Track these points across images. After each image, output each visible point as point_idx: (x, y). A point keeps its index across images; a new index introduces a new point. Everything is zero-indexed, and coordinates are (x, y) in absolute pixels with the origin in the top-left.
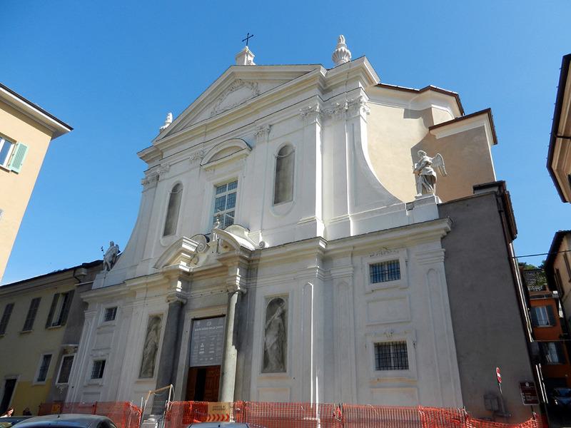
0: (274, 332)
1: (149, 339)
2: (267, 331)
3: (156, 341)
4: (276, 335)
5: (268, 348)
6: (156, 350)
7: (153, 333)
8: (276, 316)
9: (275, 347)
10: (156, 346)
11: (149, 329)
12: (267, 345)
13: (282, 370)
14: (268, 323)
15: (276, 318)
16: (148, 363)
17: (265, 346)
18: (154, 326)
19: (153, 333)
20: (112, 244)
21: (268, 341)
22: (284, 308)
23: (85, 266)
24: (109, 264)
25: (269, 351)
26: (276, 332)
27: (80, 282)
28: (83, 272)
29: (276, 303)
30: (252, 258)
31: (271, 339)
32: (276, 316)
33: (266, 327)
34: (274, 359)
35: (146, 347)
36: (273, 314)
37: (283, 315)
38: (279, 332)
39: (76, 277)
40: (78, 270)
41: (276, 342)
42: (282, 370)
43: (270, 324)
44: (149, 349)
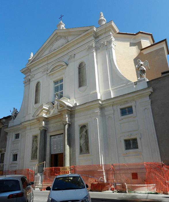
0: (83, 138)
1: (33, 145)
2: (81, 138)
4: (84, 140)
5: (82, 145)
6: (37, 148)
7: (35, 142)
8: (84, 132)
9: (84, 144)
10: (36, 147)
11: (33, 141)
12: (81, 144)
13: (88, 153)
17: (80, 144)
18: (35, 140)
19: (35, 142)
20: (14, 109)
21: (81, 142)
23: (4, 118)
24: (14, 117)
25: (82, 147)
26: (84, 139)
27: (3, 125)
28: (4, 120)
29: (83, 127)
30: (72, 110)
31: (83, 141)
32: (84, 132)
33: (80, 137)
34: (84, 148)
35: (33, 148)
38: (85, 138)
39: (1, 123)
40: (2, 120)
41: (84, 142)
42: (88, 153)
43: (82, 135)
44: (34, 148)
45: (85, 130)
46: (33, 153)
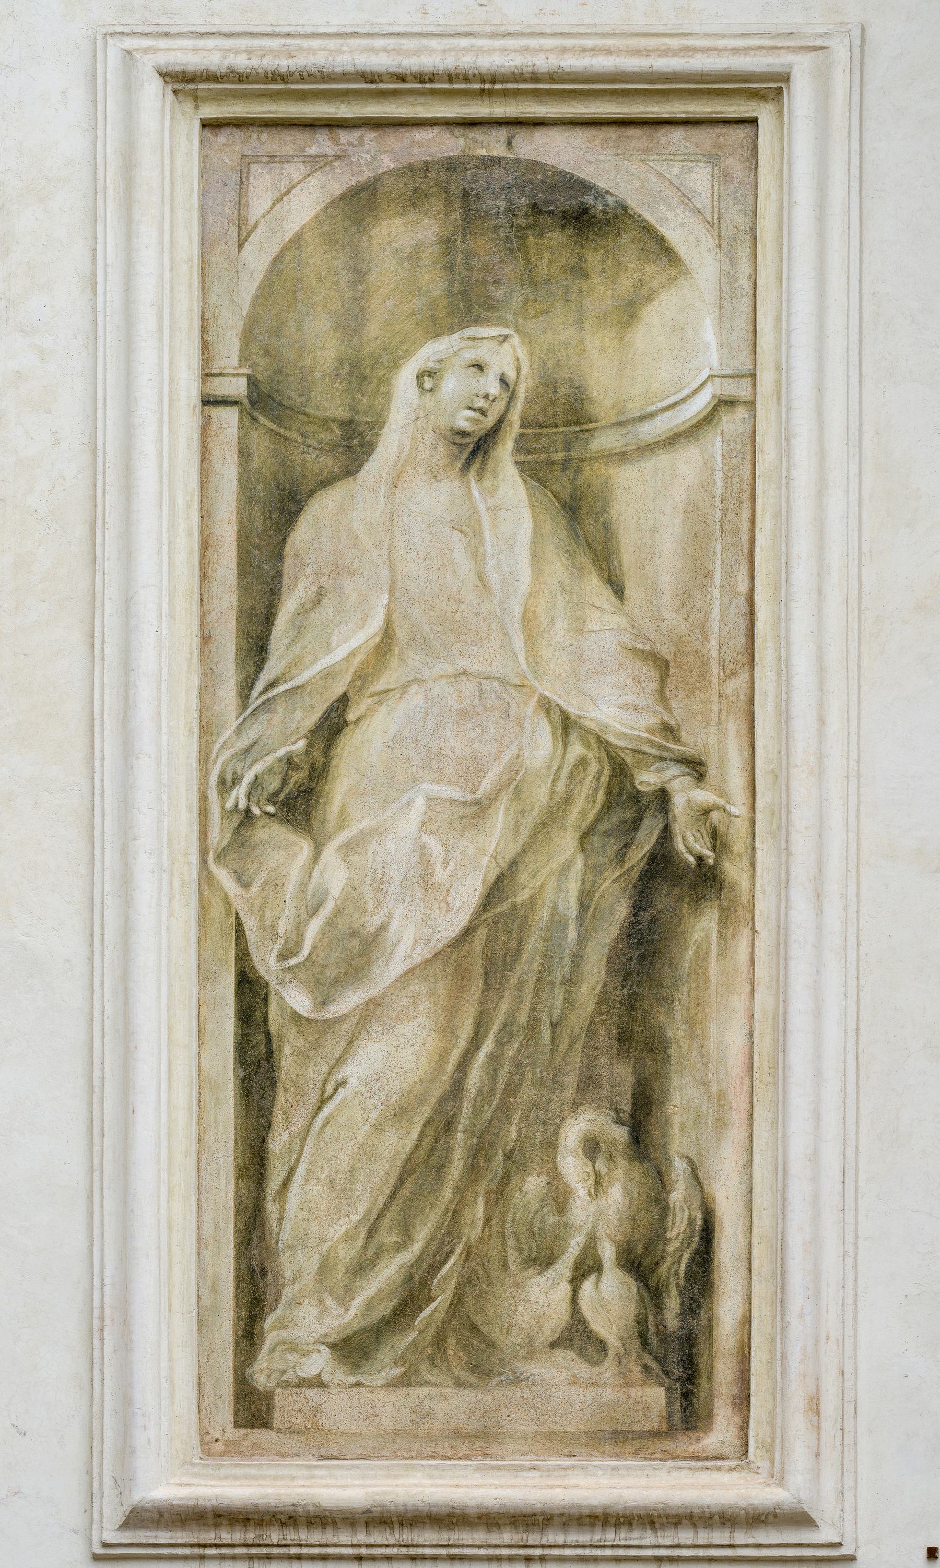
3: (617, 709)
16: (461, 1147)
44: (408, 856)
46: (382, 1066)
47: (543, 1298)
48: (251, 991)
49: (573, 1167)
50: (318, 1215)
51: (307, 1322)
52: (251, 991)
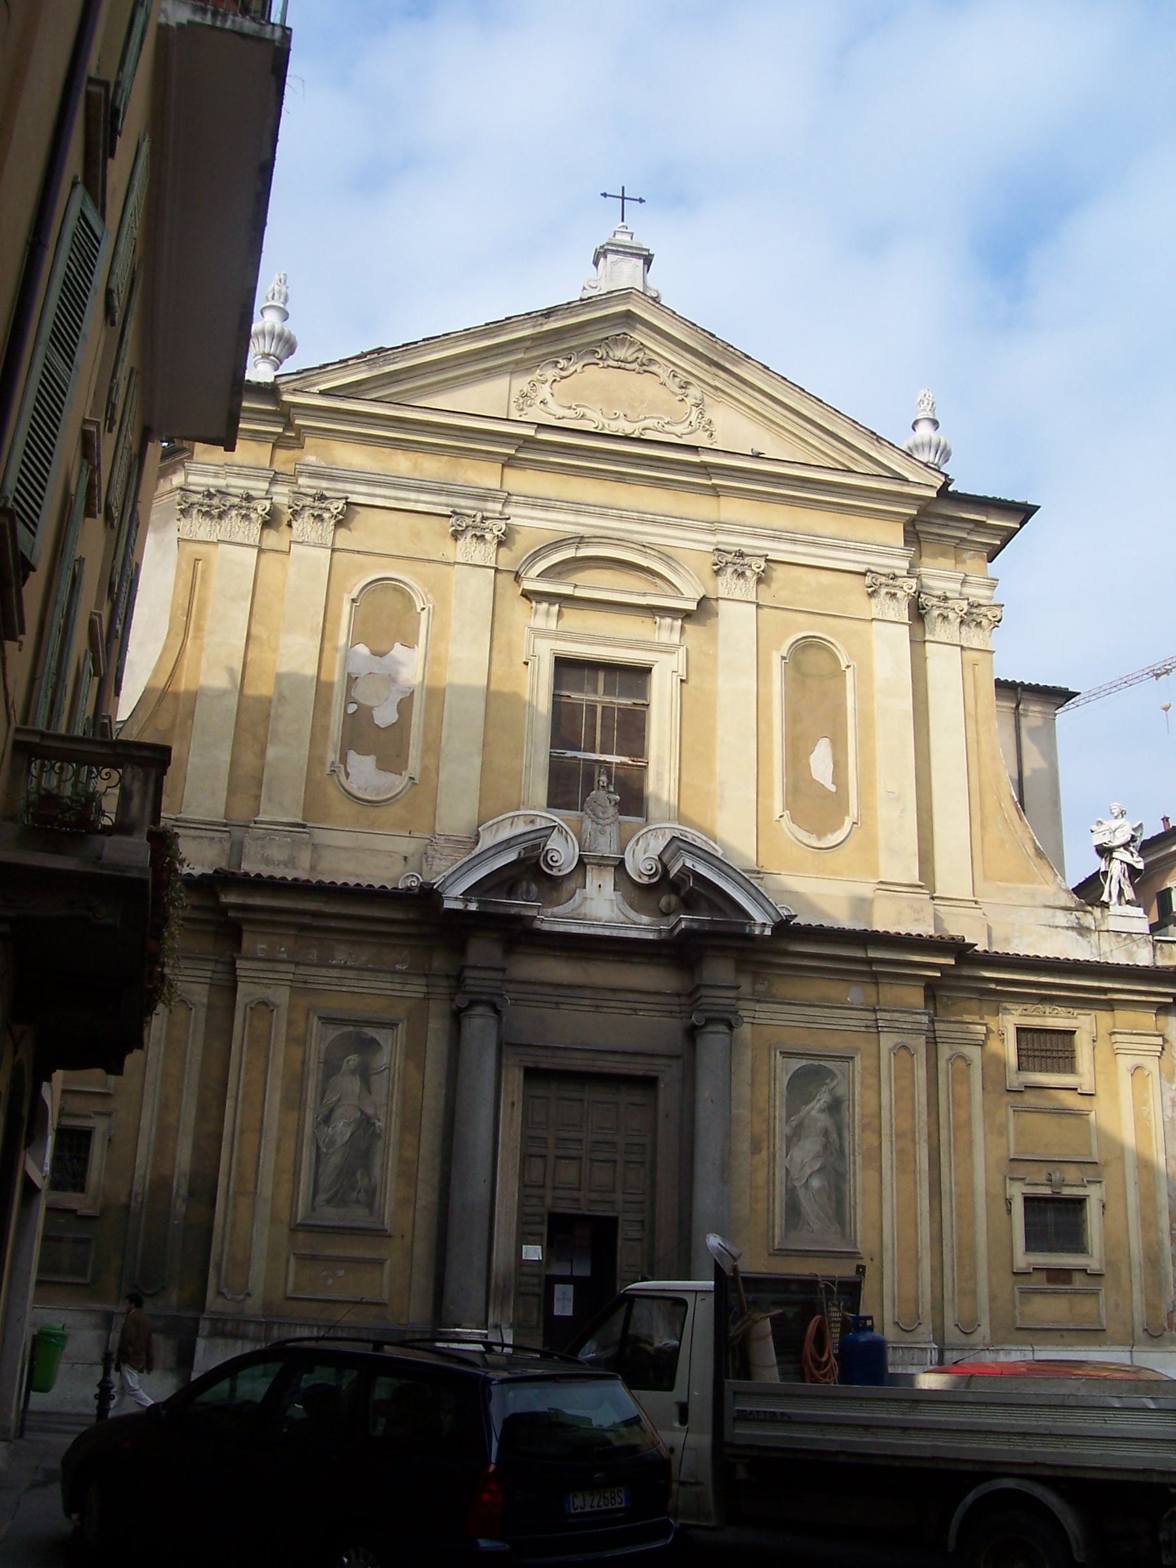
14: (794, 1124)
15: (813, 1113)
22: (841, 1091)
32: (815, 1110)
36: (807, 1103)
37: (835, 1107)
43: (800, 1126)
45: (823, 1098)
46: (335, 1160)
47: (354, 1195)
48: (318, 1148)
49: (359, 1177)
50: (325, 1181)
51: (322, 1197)
52: (318, 1148)
